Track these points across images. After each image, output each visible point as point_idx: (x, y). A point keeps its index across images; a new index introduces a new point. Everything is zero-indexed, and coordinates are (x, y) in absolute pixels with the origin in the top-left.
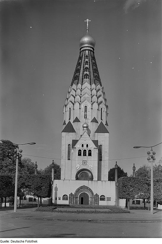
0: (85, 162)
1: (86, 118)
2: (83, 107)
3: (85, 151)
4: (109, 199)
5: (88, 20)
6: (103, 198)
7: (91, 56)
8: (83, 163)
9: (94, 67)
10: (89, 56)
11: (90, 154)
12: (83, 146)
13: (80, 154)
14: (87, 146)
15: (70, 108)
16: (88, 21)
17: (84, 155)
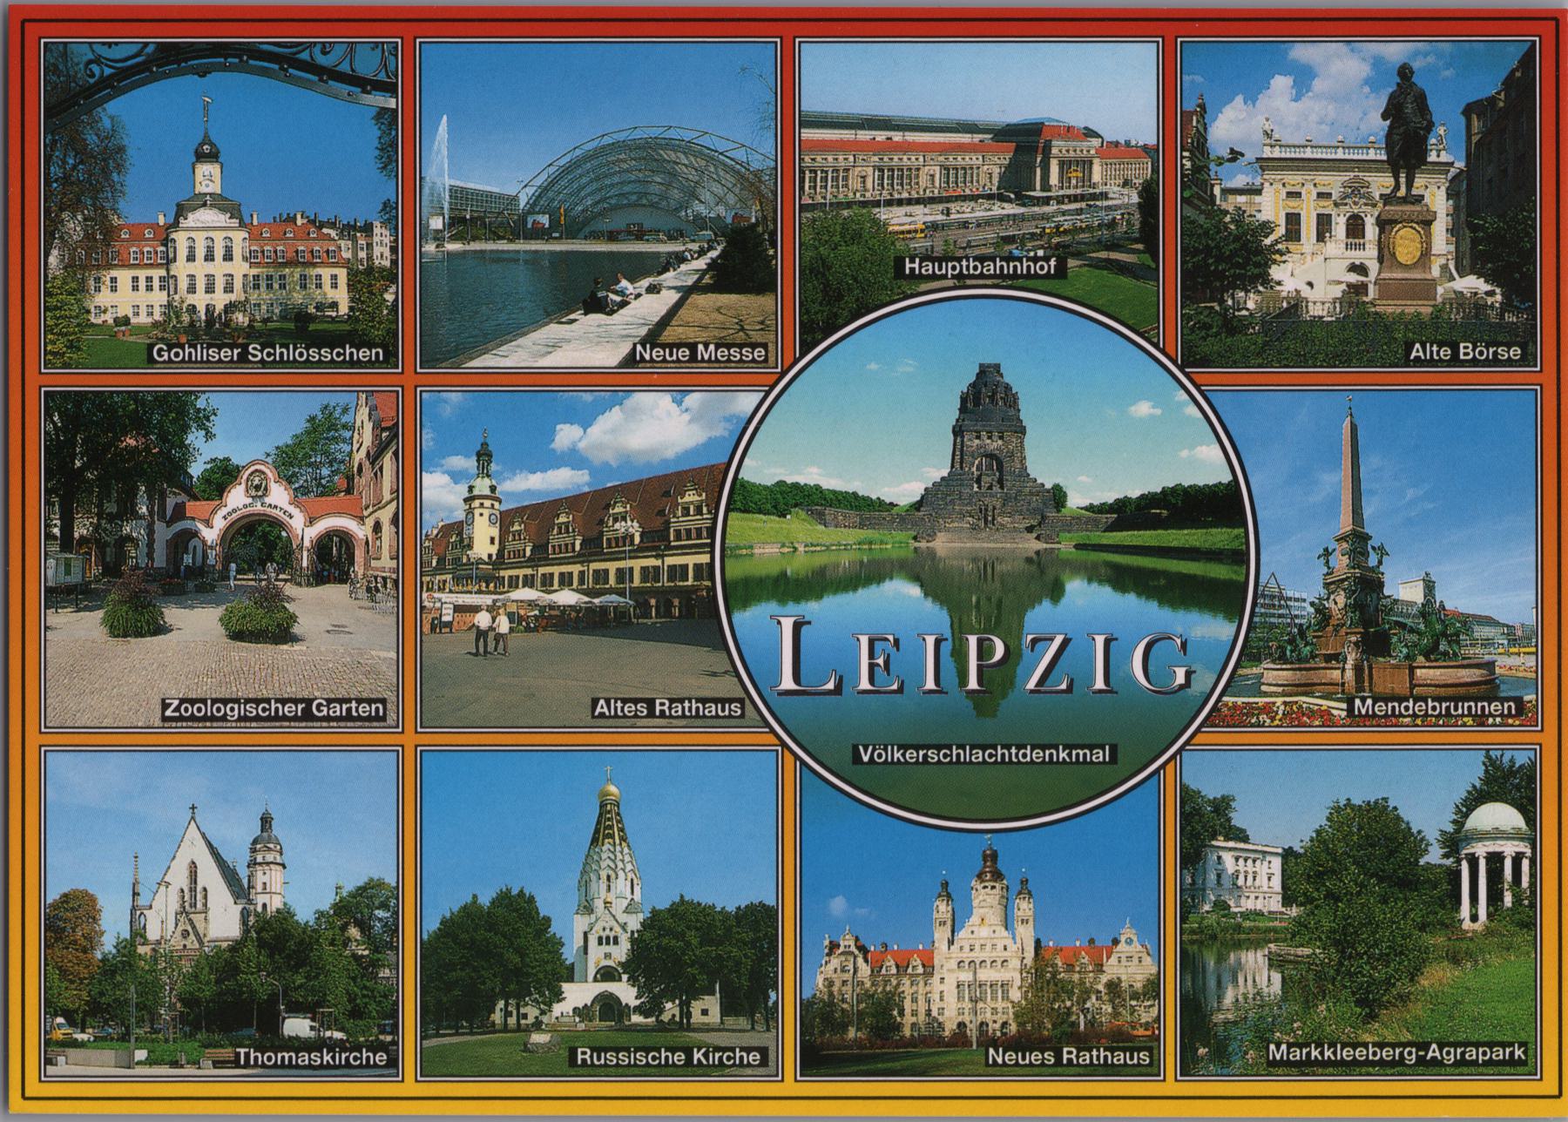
0: (608, 956)
2: (604, 874)
11: (616, 941)
13: (600, 943)
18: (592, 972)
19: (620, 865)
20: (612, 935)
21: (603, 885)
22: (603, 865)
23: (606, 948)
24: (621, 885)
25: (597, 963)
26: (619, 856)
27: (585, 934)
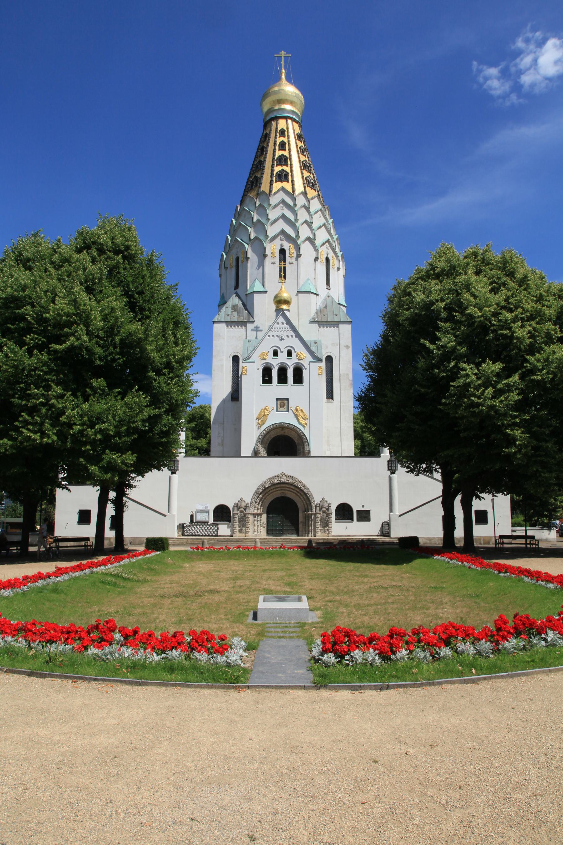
1: (285, 277)
3: (282, 371)
4: (364, 516)
5: (283, 52)
6: (344, 512)
7: (294, 130)
8: (279, 406)
9: (303, 158)
10: (288, 131)
11: (298, 378)
12: (275, 353)
14: (289, 354)
15: (238, 259)
18: (250, 436)
19: (305, 232)
20: (291, 363)
21: (272, 267)
22: (272, 231)
23: (277, 389)
24: (307, 268)
25: (262, 417)
26: (303, 216)
27: (236, 359)
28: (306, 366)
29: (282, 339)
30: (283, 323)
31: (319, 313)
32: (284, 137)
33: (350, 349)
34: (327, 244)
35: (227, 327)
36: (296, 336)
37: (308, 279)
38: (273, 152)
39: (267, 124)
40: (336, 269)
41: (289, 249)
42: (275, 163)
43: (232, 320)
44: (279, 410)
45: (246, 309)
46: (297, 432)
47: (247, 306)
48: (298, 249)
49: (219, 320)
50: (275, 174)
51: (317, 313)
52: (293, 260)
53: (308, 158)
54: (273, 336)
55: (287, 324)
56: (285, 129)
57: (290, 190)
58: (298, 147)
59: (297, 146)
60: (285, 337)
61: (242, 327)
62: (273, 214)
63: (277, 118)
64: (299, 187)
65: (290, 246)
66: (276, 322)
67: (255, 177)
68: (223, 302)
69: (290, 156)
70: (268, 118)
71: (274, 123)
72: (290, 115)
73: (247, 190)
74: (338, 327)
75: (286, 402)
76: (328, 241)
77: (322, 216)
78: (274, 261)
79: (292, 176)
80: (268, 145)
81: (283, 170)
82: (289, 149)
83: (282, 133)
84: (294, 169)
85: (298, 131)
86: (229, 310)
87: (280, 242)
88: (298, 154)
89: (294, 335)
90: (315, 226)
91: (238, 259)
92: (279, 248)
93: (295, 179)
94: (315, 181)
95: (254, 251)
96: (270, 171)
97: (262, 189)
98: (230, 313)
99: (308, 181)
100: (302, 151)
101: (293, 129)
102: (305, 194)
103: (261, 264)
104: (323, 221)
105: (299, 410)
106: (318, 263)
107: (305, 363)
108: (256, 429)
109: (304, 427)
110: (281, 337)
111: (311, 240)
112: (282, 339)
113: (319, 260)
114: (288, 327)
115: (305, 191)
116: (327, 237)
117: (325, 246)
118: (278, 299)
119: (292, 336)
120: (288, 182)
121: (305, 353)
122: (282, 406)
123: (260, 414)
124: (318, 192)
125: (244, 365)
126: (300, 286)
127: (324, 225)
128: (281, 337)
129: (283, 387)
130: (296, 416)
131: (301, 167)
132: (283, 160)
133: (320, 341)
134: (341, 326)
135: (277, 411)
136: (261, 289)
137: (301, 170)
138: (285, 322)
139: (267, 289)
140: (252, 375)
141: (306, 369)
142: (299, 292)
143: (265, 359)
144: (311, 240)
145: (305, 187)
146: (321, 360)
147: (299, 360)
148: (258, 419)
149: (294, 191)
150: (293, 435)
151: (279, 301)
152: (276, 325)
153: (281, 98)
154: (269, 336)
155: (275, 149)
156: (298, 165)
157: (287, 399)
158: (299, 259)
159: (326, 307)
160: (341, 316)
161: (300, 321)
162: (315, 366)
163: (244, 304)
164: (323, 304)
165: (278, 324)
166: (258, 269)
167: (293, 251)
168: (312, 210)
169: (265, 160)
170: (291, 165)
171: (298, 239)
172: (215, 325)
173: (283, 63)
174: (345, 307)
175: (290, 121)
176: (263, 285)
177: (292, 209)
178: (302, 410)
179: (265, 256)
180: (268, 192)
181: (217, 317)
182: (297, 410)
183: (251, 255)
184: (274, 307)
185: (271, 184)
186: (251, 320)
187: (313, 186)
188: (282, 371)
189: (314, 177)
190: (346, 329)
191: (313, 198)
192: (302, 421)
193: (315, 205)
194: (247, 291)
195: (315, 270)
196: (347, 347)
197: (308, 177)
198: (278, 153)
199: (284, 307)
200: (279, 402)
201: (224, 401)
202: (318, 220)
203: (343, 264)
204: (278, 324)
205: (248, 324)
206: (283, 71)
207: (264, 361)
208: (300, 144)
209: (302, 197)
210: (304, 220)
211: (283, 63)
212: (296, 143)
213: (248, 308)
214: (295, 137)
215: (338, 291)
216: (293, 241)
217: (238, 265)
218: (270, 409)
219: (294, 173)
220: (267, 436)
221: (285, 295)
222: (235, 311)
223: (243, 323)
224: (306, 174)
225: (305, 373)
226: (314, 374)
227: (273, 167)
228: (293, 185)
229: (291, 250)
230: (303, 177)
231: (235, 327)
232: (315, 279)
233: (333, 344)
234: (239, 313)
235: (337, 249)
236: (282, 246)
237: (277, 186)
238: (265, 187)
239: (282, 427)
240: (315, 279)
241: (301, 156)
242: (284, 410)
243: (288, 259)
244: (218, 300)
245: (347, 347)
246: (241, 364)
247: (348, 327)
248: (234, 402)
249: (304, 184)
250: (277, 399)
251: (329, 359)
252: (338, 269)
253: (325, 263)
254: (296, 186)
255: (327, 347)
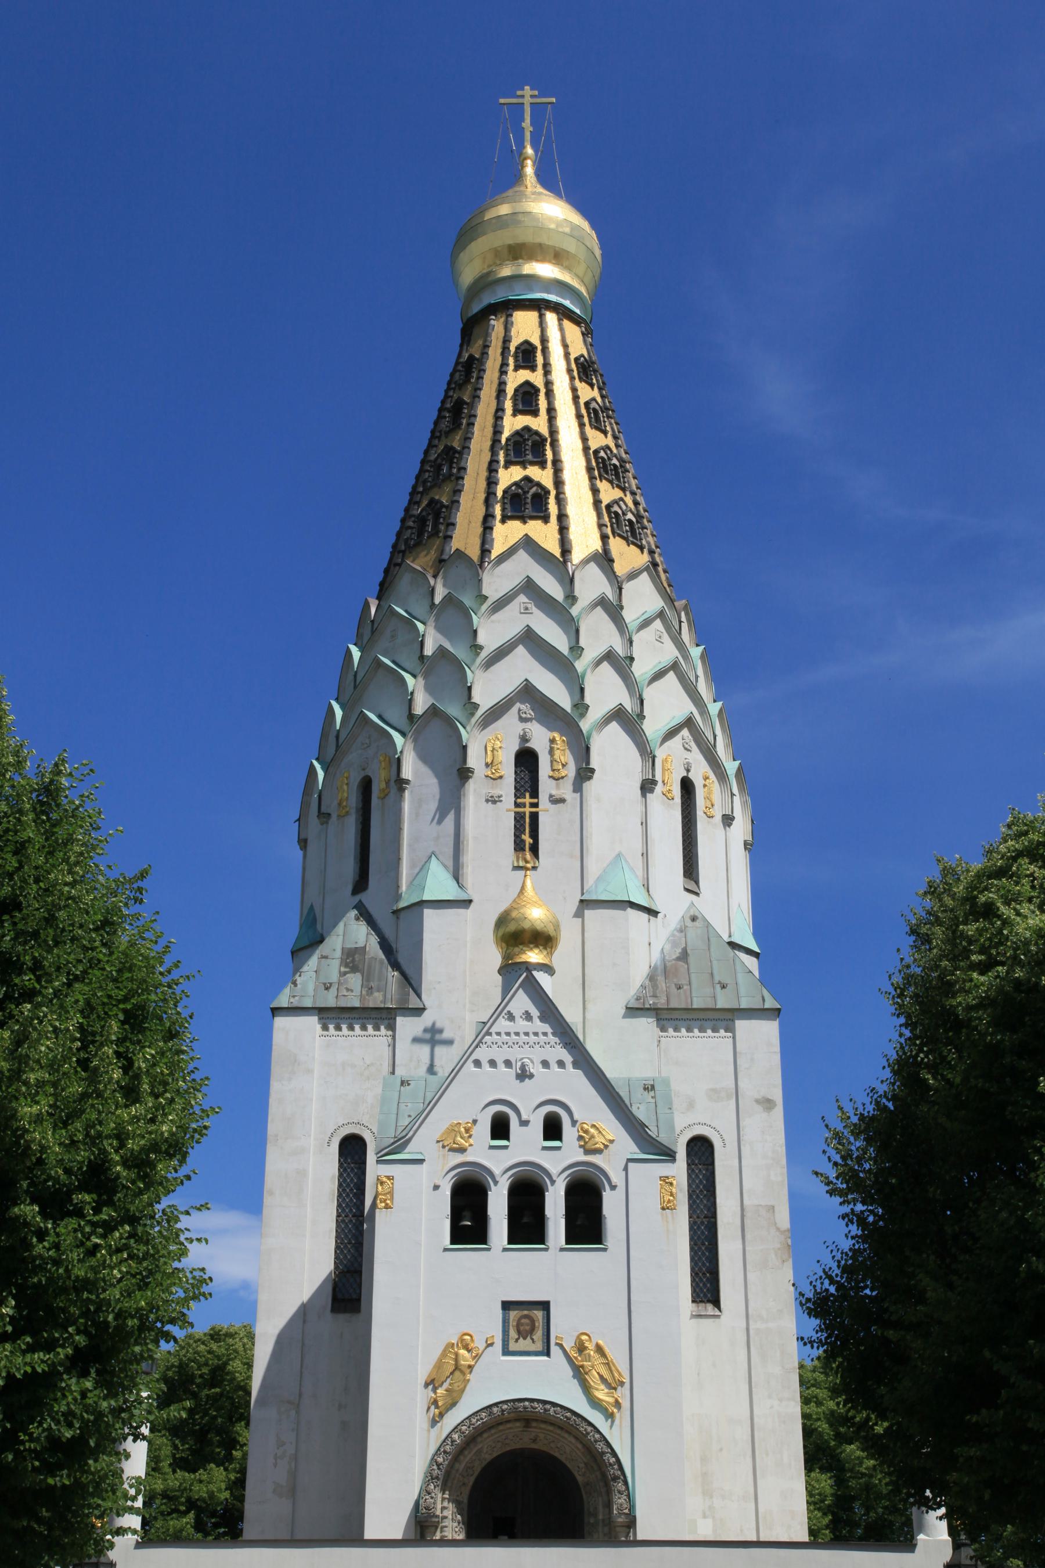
1: (535, 850)
3: (527, 1195)
7: (565, 346)
8: (513, 1334)
9: (597, 440)
10: (545, 350)
11: (586, 1225)
12: (500, 1128)
14: (552, 1129)
15: (366, 785)
16: (527, 101)
17: (514, 1237)
18: (400, 1458)
19: (605, 691)
21: (488, 816)
22: (488, 687)
23: (504, 1269)
24: (615, 820)
25: (448, 1377)
26: (598, 635)
27: (352, 1149)
28: (616, 1176)
29: (524, 1075)
30: (528, 1017)
31: (661, 979)
32: (533, 368)
33: (779, 1112)
34: (685, 732)
35: (325, 1028)
36: (576, 1065)
37: (619, 855)
38: (495, 419)
39: (473, 326)
40: (718, 818)
41: (551, 752)
42: (498, 510)
43: (343, 1003)
44: (513, 1346)
45: (396, 965)
46: (581, 1438)
47: (399, 953)
48: (582, 750)
49: (295, 1002)
50: (499, 494)
51: (652, 978)
52: (566, 790)
53: (615, 438)
54: (493, 1063)
55: (543, 1018)
56: (536, 341)
57: (553, 546)
58: (582, 401)
59: (576, 398)
60: (536, 1069)
61: (377, 1028)
62: (492, 632)
63: (507, 307)
64: (585, 537)
65: (552, 741)
66: (502, 1011)
67: (432, 502)
68: (310, 938)
69: (553, 431)
70: (476, 308)
71: (497, 324)
72: (552, 298)
73: (403, 548)
74: (730, 1029)
75: (539, 1314)
76: (689, 723)
77: (666, 638)
78: (496, 792)
79: (560, 501)
80: (476, 397)
81: (527, 479)
82: (551, 411)
83: (527, 356)
84: (567, 475)
85: (578, 348)
86: (334, 970)
87: (519, 728)
88: (581, 425)
89: (568, 1059)
90: (641, 669)
91: (366, 785)
92: (515, 747)
93: (571, 510)
94: (639, 517)
95: (424, 756)
96: (483, 484)
97: (456, 544)
98: (334, 977)
99: (616, 518)
100: (592, 416)
101: (562, 342)
102: (604, 559)
103: (451, 803)
104: (669, 652)
105: (590, 1346)
106: (655, 798)
107: (610, 1164)
108: (426, 1425)
109: (610, 1416)
110: (523, 1067)
111: (629, 721)
112: (524, 1075)
113: (659, 788)
114: (549, 1030)
115: (606, 551)
116: (685, 707)
117: (676, 742)
118: (512, 927)
119: (561, 1064)
120: (546, 519)
121: (609, 1127)
122: (525, 1331)
123: (439, 1365)
124: (651, 552)
125: (385, 1170)
126: (590, 882)
127: (675, 666)
128: (523, 1067)
129: (527, 1258)
130: (579, 1373)
131: (589, 469)
132: (530, 447)
133: (666, 1082)
134: (741, 1025)
135: (506, 1352)
136: (447, 889)
137: (592, 478)
138: (535, 1013)
139: (472, 893)
140: (412, 1210)
141: (613, 1188)
142: (585, 904)
143: (462, 1150)
144: (629, 721)
145: (604, 538)
146: (669, 1155)
147: (588, 1152)
148: (431, 1383)
149: (566, 551)
150: (566, 1451)
151: (515, 935)
152: (503, 1024)
153: (520, 240)
154: (477, 1063)
155: (500, 410)
156: (582, 463)
157: (545, 1306)
158: (587, 785)
159: (684, 956)
160: (742, 991)
161: (589, 1006)
162: (648, 1177)
163: (386, 946)
164: (674, 944)
165: (511, 1017)
166: (439, 822)
167: (566, 757)
168: (631, 615)
169: (466, 448)
170: (557, 462)
171: (582, 715)
172: (281, 1023)
173: (527, 124)
174: (756, 955)
175: (551, 318)
176: (457, 877)
177: (560, 612)
178: (599, 1349)
179: (464, 774)
180: (474, 553)
181: (287, 991)
182: (581, 1348)
183: (415, 773)
184: (495, 957)
185: (487, 527)
186: (414, 1002)
187: (633, 535)
188: (527, 1195)
189: (636, 503)
190: (761, 1038)
191: (633, 575)
192: (602, 1394)
193: (642, 598)
194: (398, 897)
195: (645, 824)
196: (767, 1104)
197: (616, 502)
198: (512, 424)
199: (534, 956)
200: (513, 1314)
201: (304, 1311)
202: (652, 651)
203: (744, 804)
204: (511, 1017)
205: (400, 1020)
206: (529, 151)
207: (459, 1158)
208: (586, 393)
209: (593, 570)
210: (600, 650)
211: (527, 124)
212: (574, 390)
213: (401, 959)
214: (569, 371)
215: (728, 899)
216: (565, 722)
217: (371, 802)
218: (479, 1344)
219: (568, 489)
220: (468, 1456)
221: (536, 914)
222: (354, 969)
223: (381, 1017)
224: (609, 493)
225: (611, 1204)
226: (646, 1206)
227: (492, 469)
228: (563, 530)
229: (557, 753)
230: (597, 503)
231: (351, 1028)
232: (645, 855)
233: (714, 1094)
234: (367, 979)
235: (722, 750)
236: (524, 739)
237: (507, 533)
238: (464, 537)
239: (523, 1414)
240: (645, 855)
241: (589, 431)
242: (533, 1348)
243: (546, 786)
244: (291, 932)
245: (767, 1104)
246: (373, 1170)
247: (769, 1030)
248: (342, 1317)
249: (601, 526)
250: (507, 1306)
251: (701, 1150)
252: (728, 820)
253: (678, 800)
254: (573, 534)
255: (691, 1105)
